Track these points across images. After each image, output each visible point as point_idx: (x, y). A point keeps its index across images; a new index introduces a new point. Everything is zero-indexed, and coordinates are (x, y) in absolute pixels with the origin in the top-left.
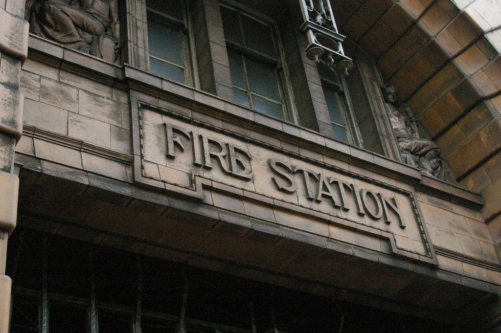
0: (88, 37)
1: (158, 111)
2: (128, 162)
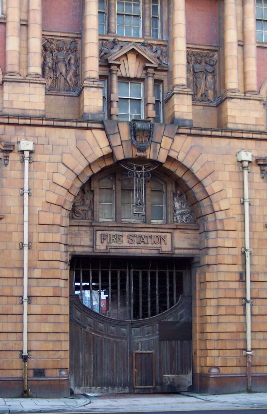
0: (85, 212)
2: (93, 247)
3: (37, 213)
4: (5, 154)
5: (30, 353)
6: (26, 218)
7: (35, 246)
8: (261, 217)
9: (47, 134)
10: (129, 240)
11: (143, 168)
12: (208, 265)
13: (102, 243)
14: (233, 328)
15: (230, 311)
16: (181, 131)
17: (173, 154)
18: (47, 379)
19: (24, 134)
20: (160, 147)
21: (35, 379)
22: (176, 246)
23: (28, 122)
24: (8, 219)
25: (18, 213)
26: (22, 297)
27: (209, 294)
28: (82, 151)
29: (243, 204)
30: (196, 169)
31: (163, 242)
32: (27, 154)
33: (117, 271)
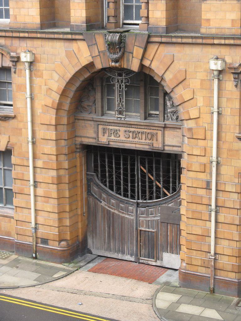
0: (90, 107)
8: (232, 126)
11: (123, 76)
14: (200, 232)
15: (196, 216)
17: (146, 63)
18: (49, 247)
30: (168, 77)
31: (155, 139)
32: (27, 65)
33: (128, 156)
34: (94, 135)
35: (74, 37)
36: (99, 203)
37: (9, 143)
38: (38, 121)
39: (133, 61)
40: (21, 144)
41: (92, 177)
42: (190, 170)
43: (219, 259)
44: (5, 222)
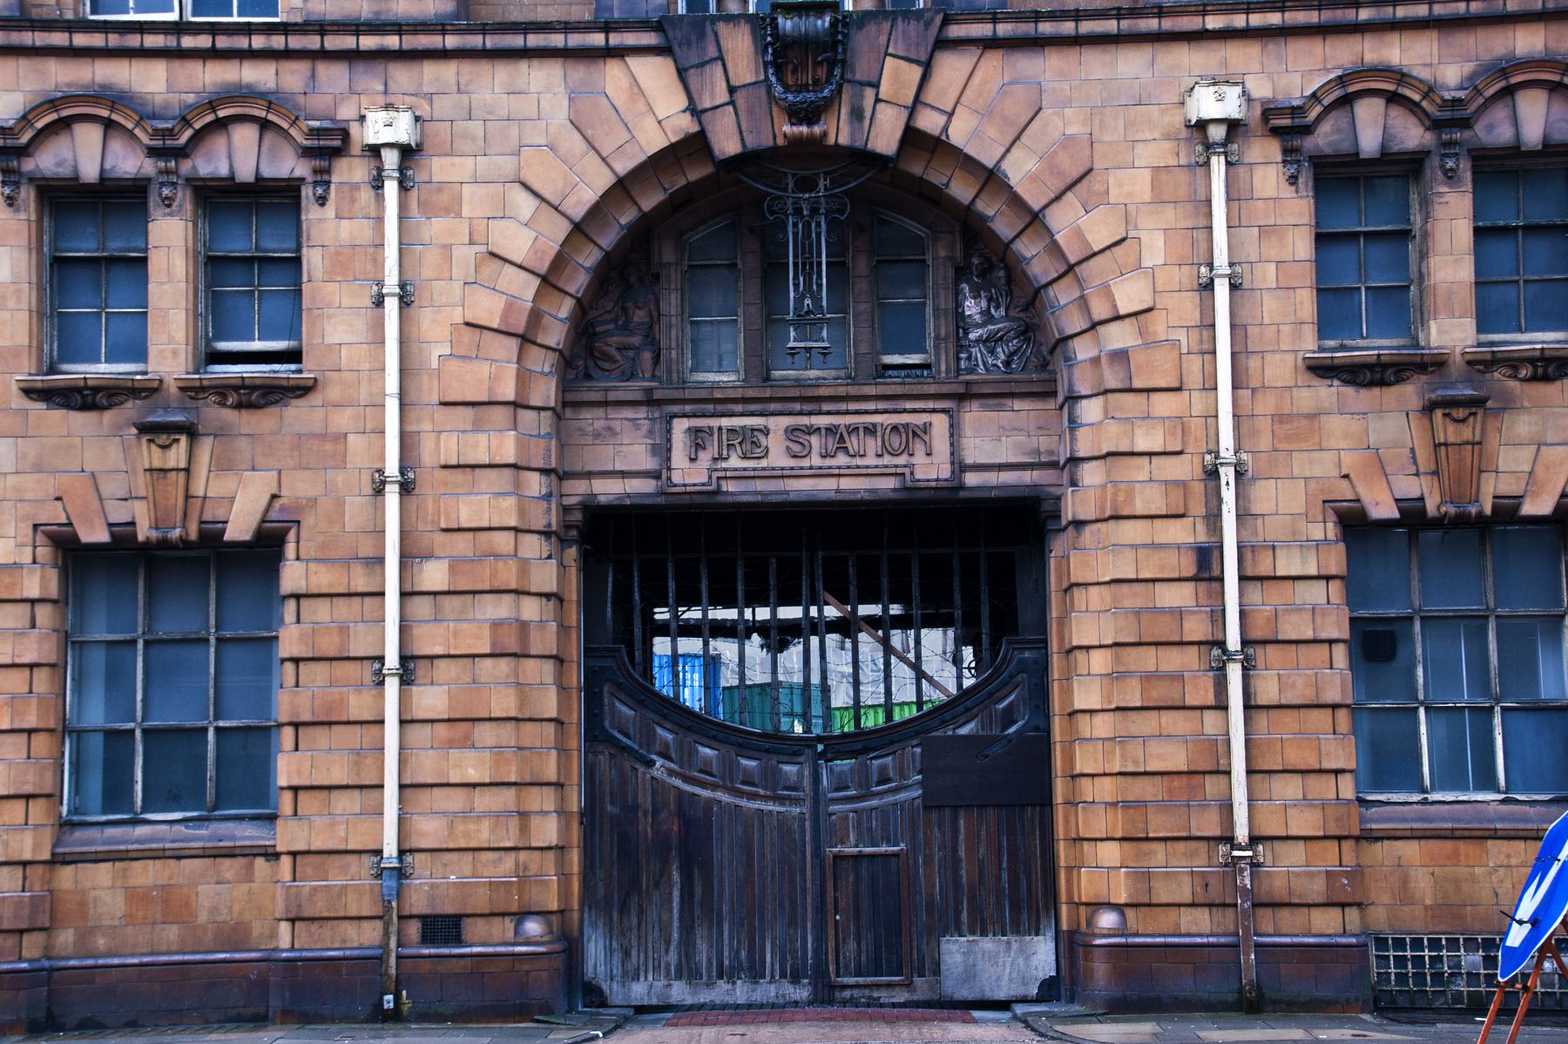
0: (631, 354)
1: (685, 416)
2: (656, 475)
3: (435, 365)
4: (317, 163)
5: (409, 858)
6: (392, 383)
7: (430, 483)
9: (462, 81)
10: (791, 445)
12: (1079, 524)
13: (692, 460)
14: (1177, 759)
15: (1160, 693)
16: (956, 31)
17: (929, 122)
18: (467, 950)
19: (381, 88)
20: (878, 100)
21: (426, 951)
22: (969, 460)
23: (392, 42)
24: (333, 393)
25: (367, 366)
26: (381, 659)
27: (1084, 630)
28: (589, 133)
29: (1209, 286)
30: (1020, 170)
31: (919, 448)
32: (391, 159)
34: (649, 463)
35: (615, 39)
36: (641, 769)
37: (277, 504)
38: (429, 392)
39: (878, 116)
40: (340, 504)
41: (608, 663)
42: (1125, 513)
43: (1269, 863)
44: (218, 883)
